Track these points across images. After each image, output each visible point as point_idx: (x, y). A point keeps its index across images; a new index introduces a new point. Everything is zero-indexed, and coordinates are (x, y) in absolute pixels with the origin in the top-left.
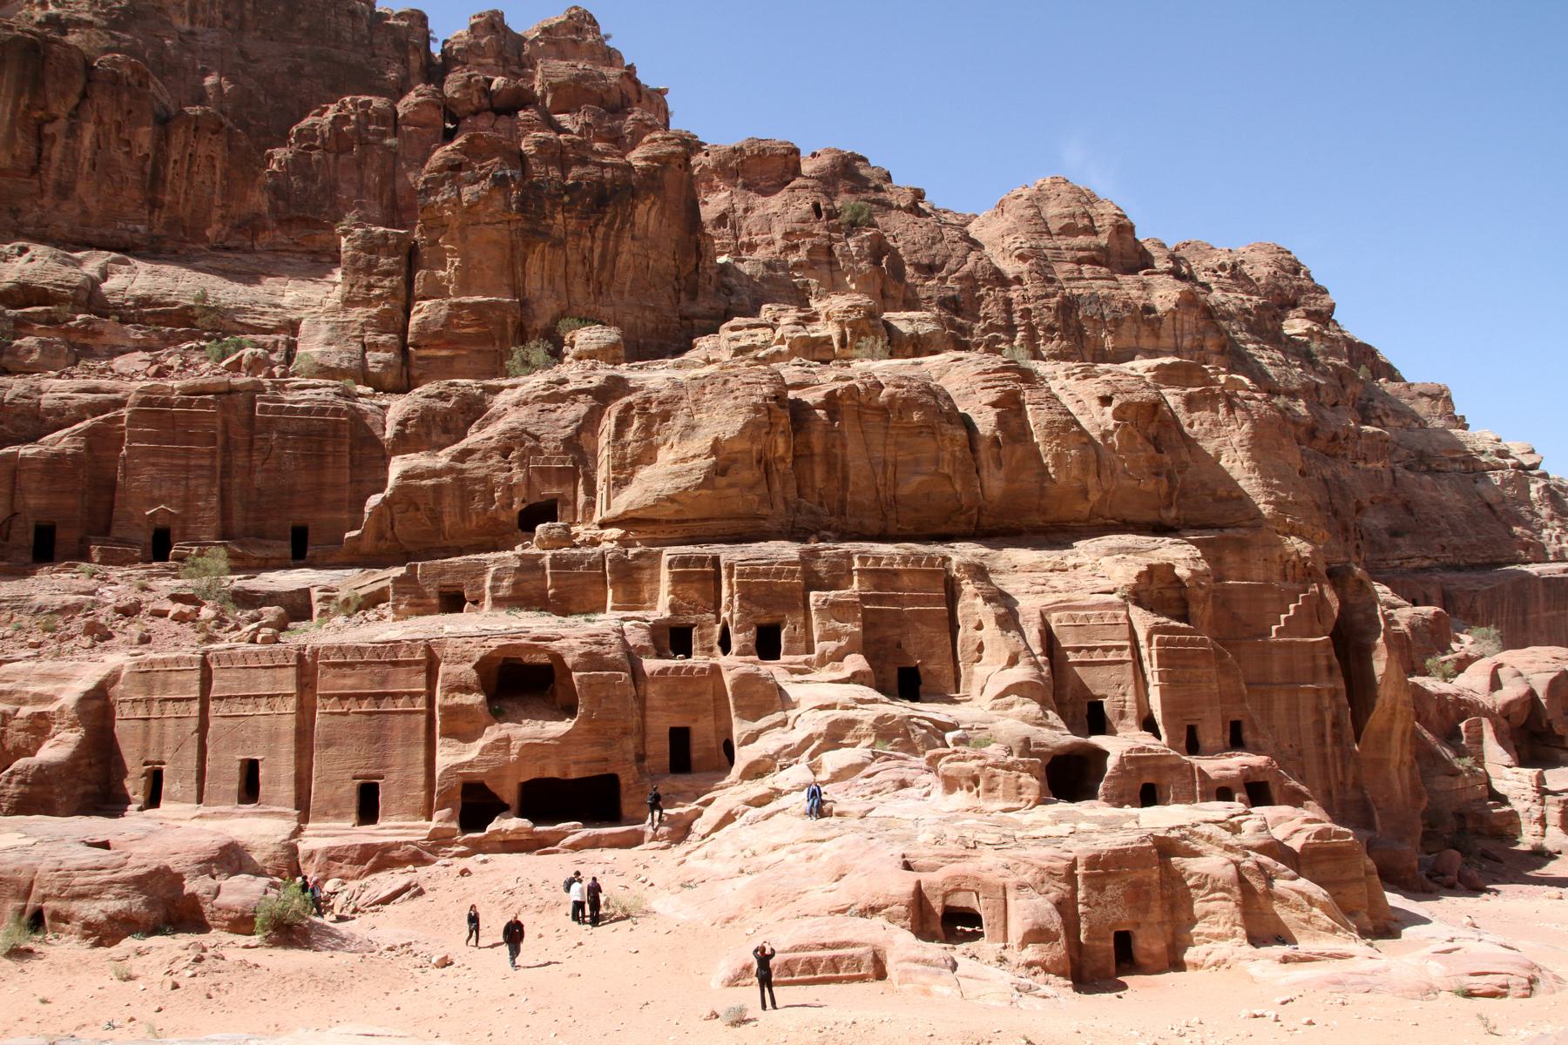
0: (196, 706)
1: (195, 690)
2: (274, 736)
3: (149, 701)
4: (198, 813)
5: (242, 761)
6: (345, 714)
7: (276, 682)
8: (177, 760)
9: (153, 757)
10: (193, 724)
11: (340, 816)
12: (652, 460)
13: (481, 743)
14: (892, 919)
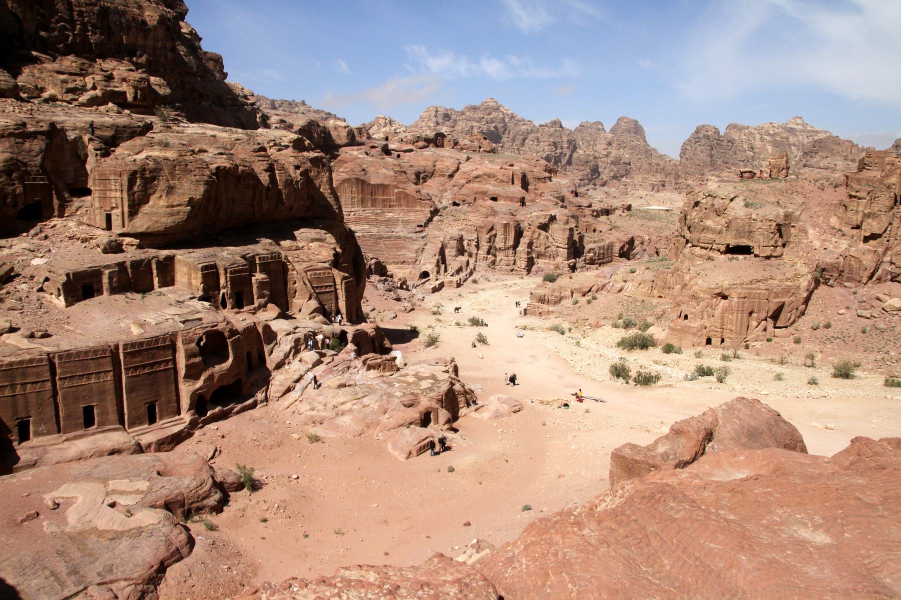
0: (49, 384)
1: (47, 376)
2: (102, 392)
3: (13, 386)
4: (64, 438)
5: (84, 408)
6: (138, 376)
7: (100, 365)
9: (22, 414)
10: (49, 394)
11: (141, 423)
12: (147, 202)
13: (203, 378)
14: (416, 424)
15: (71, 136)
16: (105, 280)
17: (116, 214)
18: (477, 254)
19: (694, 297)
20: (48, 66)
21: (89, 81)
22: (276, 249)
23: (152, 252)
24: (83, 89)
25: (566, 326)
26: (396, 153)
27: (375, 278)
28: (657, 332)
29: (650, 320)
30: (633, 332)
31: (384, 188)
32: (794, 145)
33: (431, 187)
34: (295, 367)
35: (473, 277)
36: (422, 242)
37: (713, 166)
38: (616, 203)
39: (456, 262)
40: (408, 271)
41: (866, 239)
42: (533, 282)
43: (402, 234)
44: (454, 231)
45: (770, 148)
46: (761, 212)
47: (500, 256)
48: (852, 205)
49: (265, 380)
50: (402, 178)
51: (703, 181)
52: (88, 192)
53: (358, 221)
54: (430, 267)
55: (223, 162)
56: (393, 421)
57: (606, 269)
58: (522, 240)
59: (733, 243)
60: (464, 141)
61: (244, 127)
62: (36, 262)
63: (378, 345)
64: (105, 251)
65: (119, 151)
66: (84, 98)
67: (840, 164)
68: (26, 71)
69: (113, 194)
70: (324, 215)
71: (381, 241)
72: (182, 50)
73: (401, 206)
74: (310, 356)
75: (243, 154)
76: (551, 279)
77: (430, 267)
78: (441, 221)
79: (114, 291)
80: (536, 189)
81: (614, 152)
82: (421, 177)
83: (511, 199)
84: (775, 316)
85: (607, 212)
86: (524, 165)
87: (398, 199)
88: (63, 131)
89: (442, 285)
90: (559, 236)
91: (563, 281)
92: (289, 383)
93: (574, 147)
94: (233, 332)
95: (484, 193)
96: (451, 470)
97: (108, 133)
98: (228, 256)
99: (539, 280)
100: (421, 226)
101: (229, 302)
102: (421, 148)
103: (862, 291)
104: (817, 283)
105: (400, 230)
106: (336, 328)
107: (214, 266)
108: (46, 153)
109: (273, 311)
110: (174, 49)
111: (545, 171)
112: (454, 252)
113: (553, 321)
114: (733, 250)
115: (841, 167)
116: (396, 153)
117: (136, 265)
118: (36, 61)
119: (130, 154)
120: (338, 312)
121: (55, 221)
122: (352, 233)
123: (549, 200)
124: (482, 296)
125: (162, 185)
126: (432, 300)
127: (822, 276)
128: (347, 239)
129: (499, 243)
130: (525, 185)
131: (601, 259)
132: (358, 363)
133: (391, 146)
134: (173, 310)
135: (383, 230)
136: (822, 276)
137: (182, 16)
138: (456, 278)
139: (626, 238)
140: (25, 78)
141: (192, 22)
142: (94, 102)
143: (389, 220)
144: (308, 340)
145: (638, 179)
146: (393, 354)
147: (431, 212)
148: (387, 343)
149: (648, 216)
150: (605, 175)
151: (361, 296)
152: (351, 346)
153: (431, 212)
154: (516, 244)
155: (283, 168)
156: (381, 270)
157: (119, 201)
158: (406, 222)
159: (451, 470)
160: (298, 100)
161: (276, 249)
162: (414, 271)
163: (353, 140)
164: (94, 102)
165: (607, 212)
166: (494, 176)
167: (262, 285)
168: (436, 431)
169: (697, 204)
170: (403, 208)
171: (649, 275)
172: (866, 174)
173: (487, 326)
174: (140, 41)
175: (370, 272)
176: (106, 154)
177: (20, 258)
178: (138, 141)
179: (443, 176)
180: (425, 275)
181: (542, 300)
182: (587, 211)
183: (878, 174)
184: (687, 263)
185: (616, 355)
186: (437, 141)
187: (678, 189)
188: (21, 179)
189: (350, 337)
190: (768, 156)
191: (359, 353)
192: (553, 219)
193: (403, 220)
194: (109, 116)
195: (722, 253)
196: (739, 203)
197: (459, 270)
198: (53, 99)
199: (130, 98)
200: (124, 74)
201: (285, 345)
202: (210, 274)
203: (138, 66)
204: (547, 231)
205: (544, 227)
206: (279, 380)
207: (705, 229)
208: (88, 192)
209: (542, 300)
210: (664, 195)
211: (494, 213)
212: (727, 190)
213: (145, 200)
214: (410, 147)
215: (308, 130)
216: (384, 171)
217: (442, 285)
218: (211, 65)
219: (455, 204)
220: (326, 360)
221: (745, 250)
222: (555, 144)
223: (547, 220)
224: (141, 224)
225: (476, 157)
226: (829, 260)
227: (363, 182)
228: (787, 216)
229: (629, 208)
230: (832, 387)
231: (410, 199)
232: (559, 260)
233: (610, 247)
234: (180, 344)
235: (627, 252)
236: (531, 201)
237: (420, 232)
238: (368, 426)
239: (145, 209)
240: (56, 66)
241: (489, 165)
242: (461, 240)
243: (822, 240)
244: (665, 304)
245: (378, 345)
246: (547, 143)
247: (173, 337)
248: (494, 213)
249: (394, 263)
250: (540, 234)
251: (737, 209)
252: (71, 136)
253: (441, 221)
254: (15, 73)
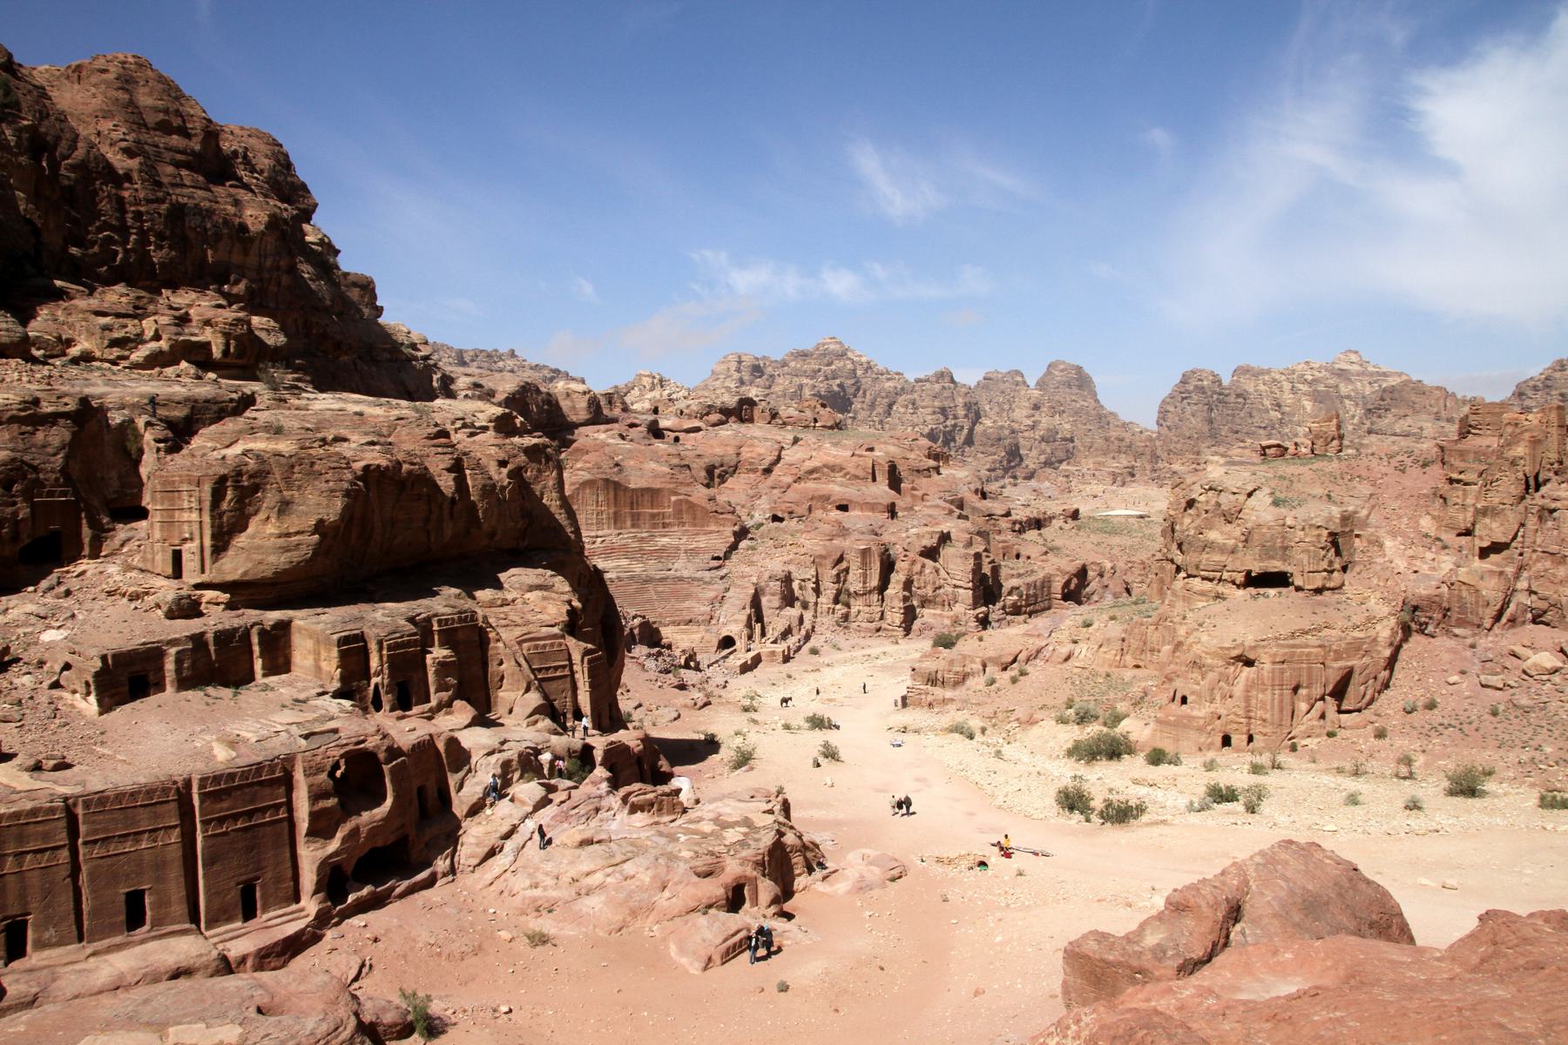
0: (65, 853)
1: (62, 838)
2: (160, 865)
4: (89, 951)
5: (128, 894)
6: (225, 834)
7: (156, 817)
8: (48, 906)
10: (65, 871)
11: (229, 920)
12: (245, 528)
13: (339, 835)
14: (719, 908)
15: (116, 418)
16: (170, 665)
17: (190, 551)
18: (816, 604)
19: (1196, 664)
20: (81, 303)
21: (148, 326)
22: (468, 604)
23: (251, 615)
24: (139, 340)
25: (975, 723)
26: (673, 435)
27: (640, 651)
28: (1134, 728)
29: (1121, 707)
30: (1094, 729)
31: (653, 494)
32: (1348, 397)
33: (734, 490)
34: (502, 813)
35: (812, 643)
36: (720, 586)
37: (1214, 437)
38: (1053, 508)
39: (780, 619)
40: (697, 637)
41: (1484, 553)
42: (916, 649)
43: (686, 574)
44: (776, 564)
45: (1308, 405)
46: (1301, 513)
47: (857, 605)
48: (1456, 494)
49: (450, 837)
50: (684, 476)
51: (1198, 465)
52: (143, 514)
53: (609, 552)
54: (735, 629)
55: (375, 457)
56: (678, 904)
57: (1041, 622)
58: (894, 577)
59: (1257, 568)
60: (788, 411)
61: (411, 397)
62: (49, 636)
63: (648, 768)
64: (170, 615)
65: (196, 442)
66: (138, 355)
67: (1429, 427)
68: (44, 312)
69: (185, 516)
70: (552, 545)
71: (650, 586)
72: (306, 270)
73: (683, 524)
74: (527, 790)
75: (410, 443)
76: (946, 642)
77: (735, 629)
78: (753, 548)
79: (184, 684)
80: (914, 489)
81: (1045, 422)
82: (715, 474)
83: (872, 507)
84: (1339, 692)
85: (1038, 524)
86: (892, 449)
87: (678, 513)
88: (102, 411)
89: (757, 660)
90: (956, 567)
91: (967, 646)
92: (493, 840)
93: (976, 415)
94: (393, 752)
95: (826, 498)
96: (784, 988)
97: (179, 413)
98: (383, 619)
99: (926, 644)
100: (718, 558)
101: (386, 700)
102: (714, 425)
103: (1485, 642)
104: (1407, 631)
105: (682, 567)
106: (575, 741)
107: (361, 638)
108: (72, 448)
109: (463, 712)
110: (293, 270)
111: (929, 457)
112: (776, 602)
113: (953, 716)
114: (1258, 581)
115: (1431, 432)
116: (673, 435)
117: (224, 637)
118: (60, 295)
119: (214, 448)
120: (578, 715)
121: (85, 565)
122: (598, 574)
123: (937, 506)
124: (827, 677)
125: (270, 498)
126: (742, 686)
127: (1415, 619)
128: (590, 584)
129: (854, 583)
130: (895, 482)
131: (1032, 604)
132: (614, 801)
133: (663, 423)
134: (288, 716)
135: (652, 568)
136: (1415, 619)
137: (307, 215)
138: (781, 647)
139: (1072, 568)
140: (43, 323)
141: (324, 225)
142: (157, 361)
143: (663, 549)
144: (529, 763)
145: (1087, 464)
146: (676, 783)
147: (735, 533)
148: (664, 765)
149: (1109, 527)
150: (1032, 460)
151: (617, 684)
152: (600, 772)
153: (735, 533)
154: (883, 585)
155: (478, 465)
156: (650, 635)
157: (196, 527)
158: (692, 553)
159: (784, 988)
160: (503, 349)
161: (468, 604)
162: (708, 636)
163: (597, 416)
164: (157, 361)
165: (1038, 524)
166: (842, 469)
167: (443, 667)
168: (752, 917)
169: (1191, 504)
170: (687, 527)
171: (1115, 630)
172: (1473, 442)
173: (837, 729)
174: (236, 258)
175: (632, 641)
176: (174, 448)
177: (21, 631)
178: (230, 425)
179: (754, 471)
180: (727, 642)
181: (932, 680)
182: (1004, 524)
183: (1493, 442)
184: (1180, 606)
185: (1066, 772)
186: (742, 411)
187: (1157, 479)
188: (28, 495)
189: (598, 755)
190: (1306, 420)
191: (615, 784)
192: (945, 538)
193: (687, 548)
194: (182, 384)
195: (1238, 587)
196: (1262, 500)
197: (787, 633)
198: (87, 357)
199: (217, 352)
200: (207, 314)
201: (484, 774)
202: (353, 652)
203: (231, 299)
204: (935, 560)
205: (931, 553)
206: (475, 835)
207: (1208, 546)
208: (143, 514)
209: (932, 680)
210: (1136, 490)
211: (843, 532)
212: (1239, 479)
213: (240, 525)
214: (697, 423)
215: (521, 400)
216: (653, 465)
217: (757, 660)
218: (354, 294)
219: (776, 518)
220: (557, 797)
221: (1278, 580)
222: (943, 411)
223: (935, 540)
224: (234, 566)
225: (809, 437)
226: (1423, 590)
227: (617, 485)
228: (1346, 519)
229: (1075, 515)
230: (1448, 812)
231: (699, 515)
232: (959, 609)
233: (1046, 583)
234: (299, 775)
235: (1075, 591)
236: (905, 509)
237: (717, 568)
238: (634, 913)
239: (241, 540)
240: (94, 302)
241: (831, 450)
242: (788, 580)
243: (1409, 557)
244: (1147, 679)
245: (648, 768)
247: (289, 760)
248: (843, 532)
249: (674, 623)
250: (923, 566)
251: (1260, 510)
252: (116, 418)
253: (753, 548)
254: (25, 317)
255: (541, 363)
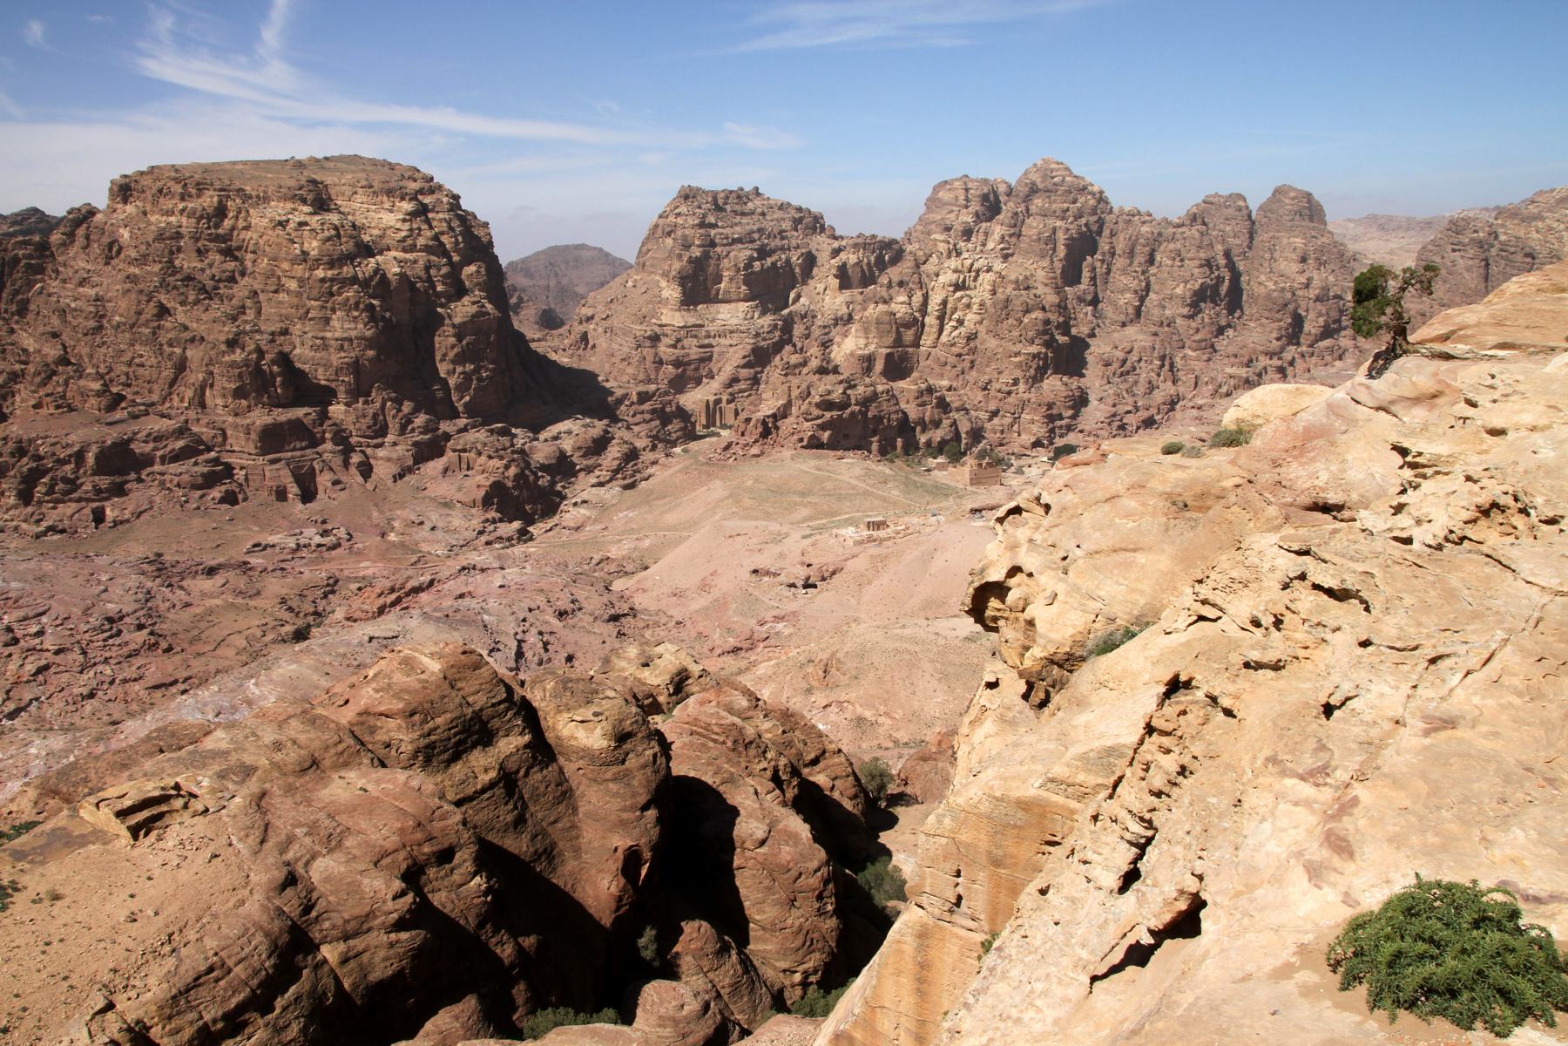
81: (1318, 278)
160: (748, 188)
222: (1209, 264)
246: (1197, 263)
255: (785, 199)
